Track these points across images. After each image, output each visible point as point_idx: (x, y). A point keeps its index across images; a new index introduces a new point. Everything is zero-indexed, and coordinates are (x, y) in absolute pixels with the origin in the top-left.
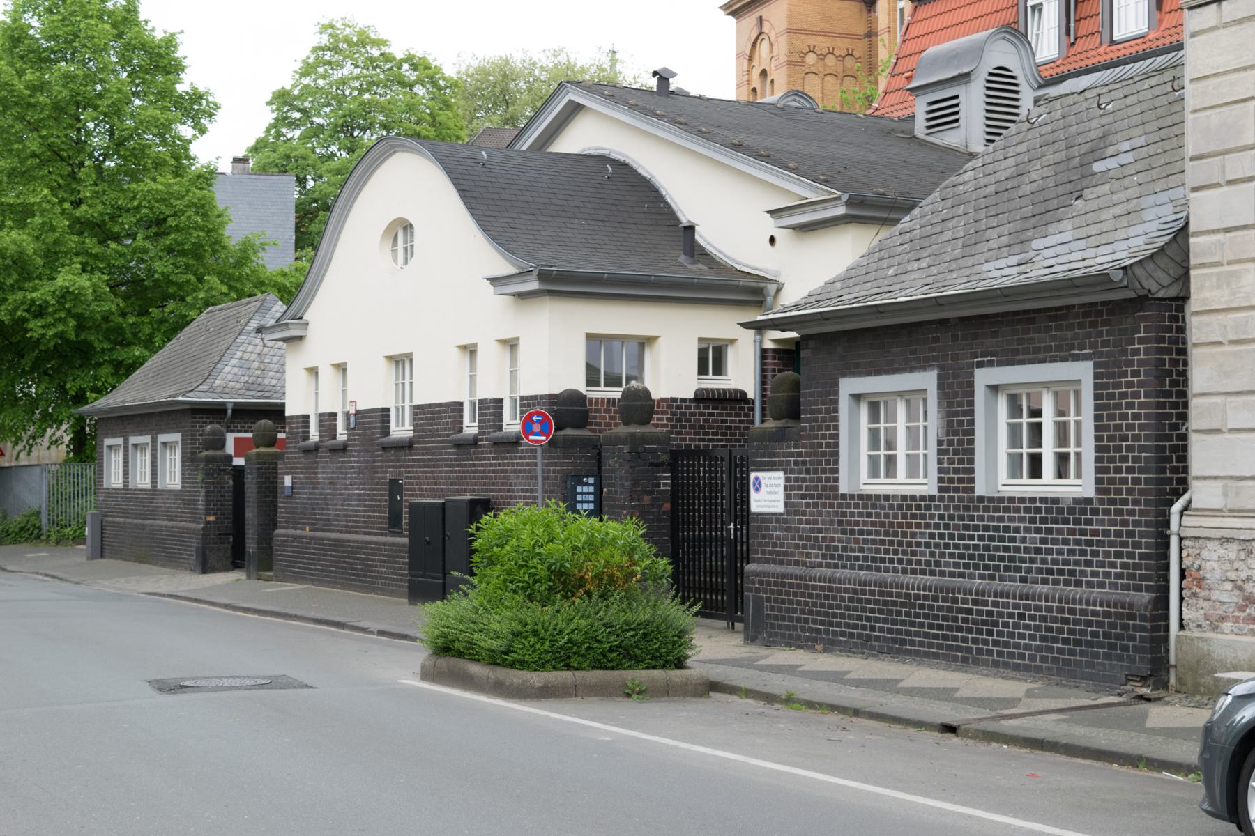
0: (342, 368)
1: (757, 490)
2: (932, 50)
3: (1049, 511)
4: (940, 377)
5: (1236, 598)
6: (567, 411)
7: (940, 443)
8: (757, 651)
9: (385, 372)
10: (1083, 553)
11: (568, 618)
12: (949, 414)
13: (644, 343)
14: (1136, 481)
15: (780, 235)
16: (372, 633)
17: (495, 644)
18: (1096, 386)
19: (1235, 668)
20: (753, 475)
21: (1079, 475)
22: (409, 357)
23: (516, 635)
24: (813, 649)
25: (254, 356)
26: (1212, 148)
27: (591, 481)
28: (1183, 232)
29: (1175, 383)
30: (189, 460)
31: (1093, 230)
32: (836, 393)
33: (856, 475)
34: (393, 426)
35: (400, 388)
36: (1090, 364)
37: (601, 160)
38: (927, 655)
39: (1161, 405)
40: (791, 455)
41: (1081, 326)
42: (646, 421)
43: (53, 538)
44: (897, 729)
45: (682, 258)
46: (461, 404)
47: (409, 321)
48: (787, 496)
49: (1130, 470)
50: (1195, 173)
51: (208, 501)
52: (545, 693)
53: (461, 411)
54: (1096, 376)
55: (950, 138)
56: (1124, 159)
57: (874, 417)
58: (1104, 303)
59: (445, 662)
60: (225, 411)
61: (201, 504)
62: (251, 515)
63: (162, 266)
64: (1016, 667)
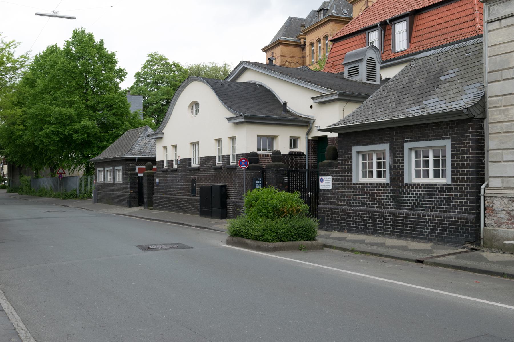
0: (175, 147)
1: (322, 182)
2: (349, 53)
3: (434, 188)
4: (390, 146)
5: (507, 216)
6: (252, 158)
7: (391, 166)
8: (328, 233)
9: (190, 148)
10: (447, 202)
11: (280, 224)
12: (394, 157)
13: (275, 137)
14: (468, 178)
15: (314, 105)
16: (193, 227)
17: (257, 233)
18: (452, 148)
19: (508, 240)
20: (320, 177)
21: (384, 177)
22: (198, 143)
23: (264, 230)
24: (343, 232)
25: (143, 144)
26: (497, 69)
27: (260, 179)
28: (484, 97)
29: (481, 146)
30: (125, 174)
31: (447, 97)
32: (351, 151)
33: (358, 177)
34: (192, 163)
35: (194, 153)
36: (450, 140)
37: (253, 85)
38: (386, 234)
39: (477, 153)
40: (335, 171)
41: (446, 128)
42: (279, 161)
43: (81, 197)
44: (398, 261)
45: (283, 112)
46: (216, 157)
47: (199, 132)
48: (333, 184)
49: (465, 175)
50: (487, 77)
51: (131, 187)
52: (275, 250)
53: (216, 159)
54: (452, 144)
55: (356, 78)
56: (451, 75)
57: (364, 158)
58: (455, 121)
59: (236, 239)
60: (135, 160)
61: (129, 187)
62: (145, 190)
63: (112, 119)
64: (421, 238)
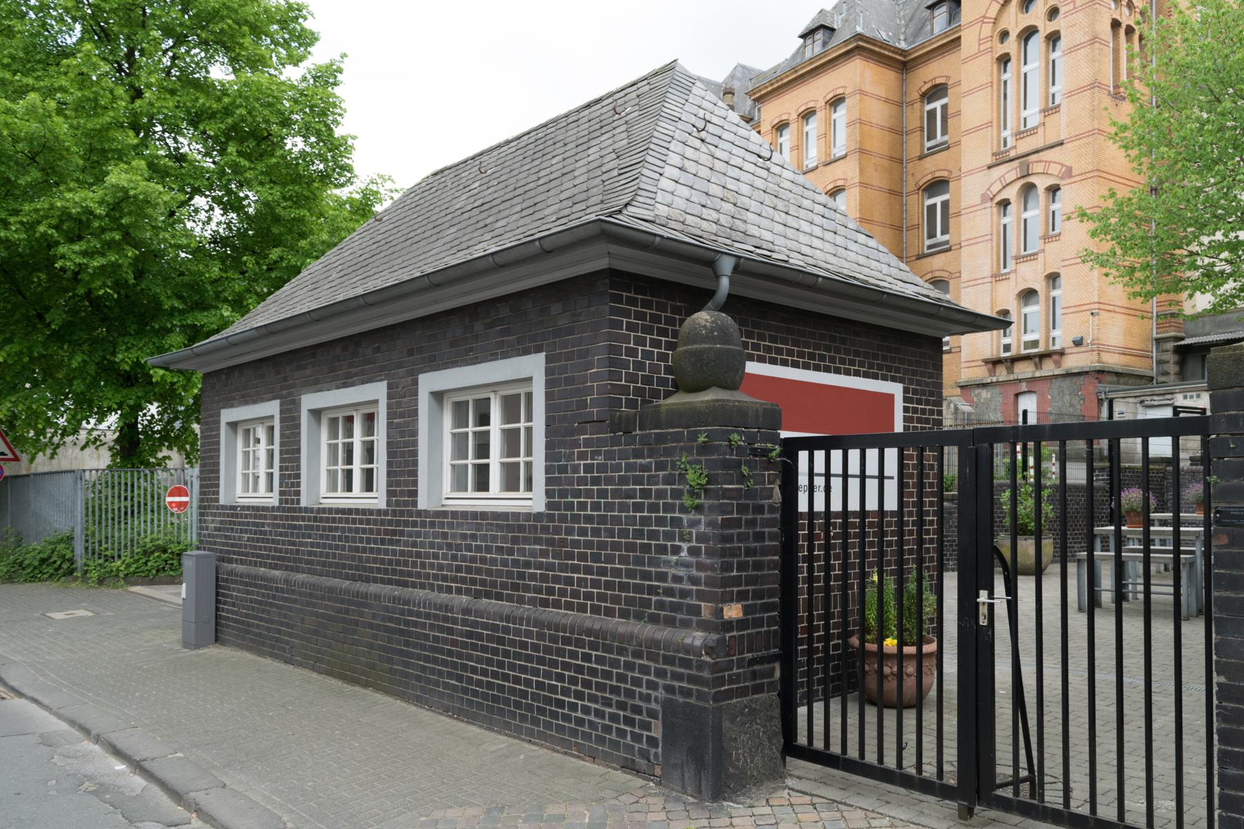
43: (94, 575)
61: (683, 562)
